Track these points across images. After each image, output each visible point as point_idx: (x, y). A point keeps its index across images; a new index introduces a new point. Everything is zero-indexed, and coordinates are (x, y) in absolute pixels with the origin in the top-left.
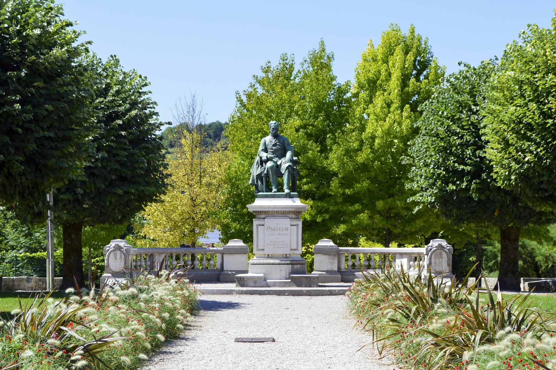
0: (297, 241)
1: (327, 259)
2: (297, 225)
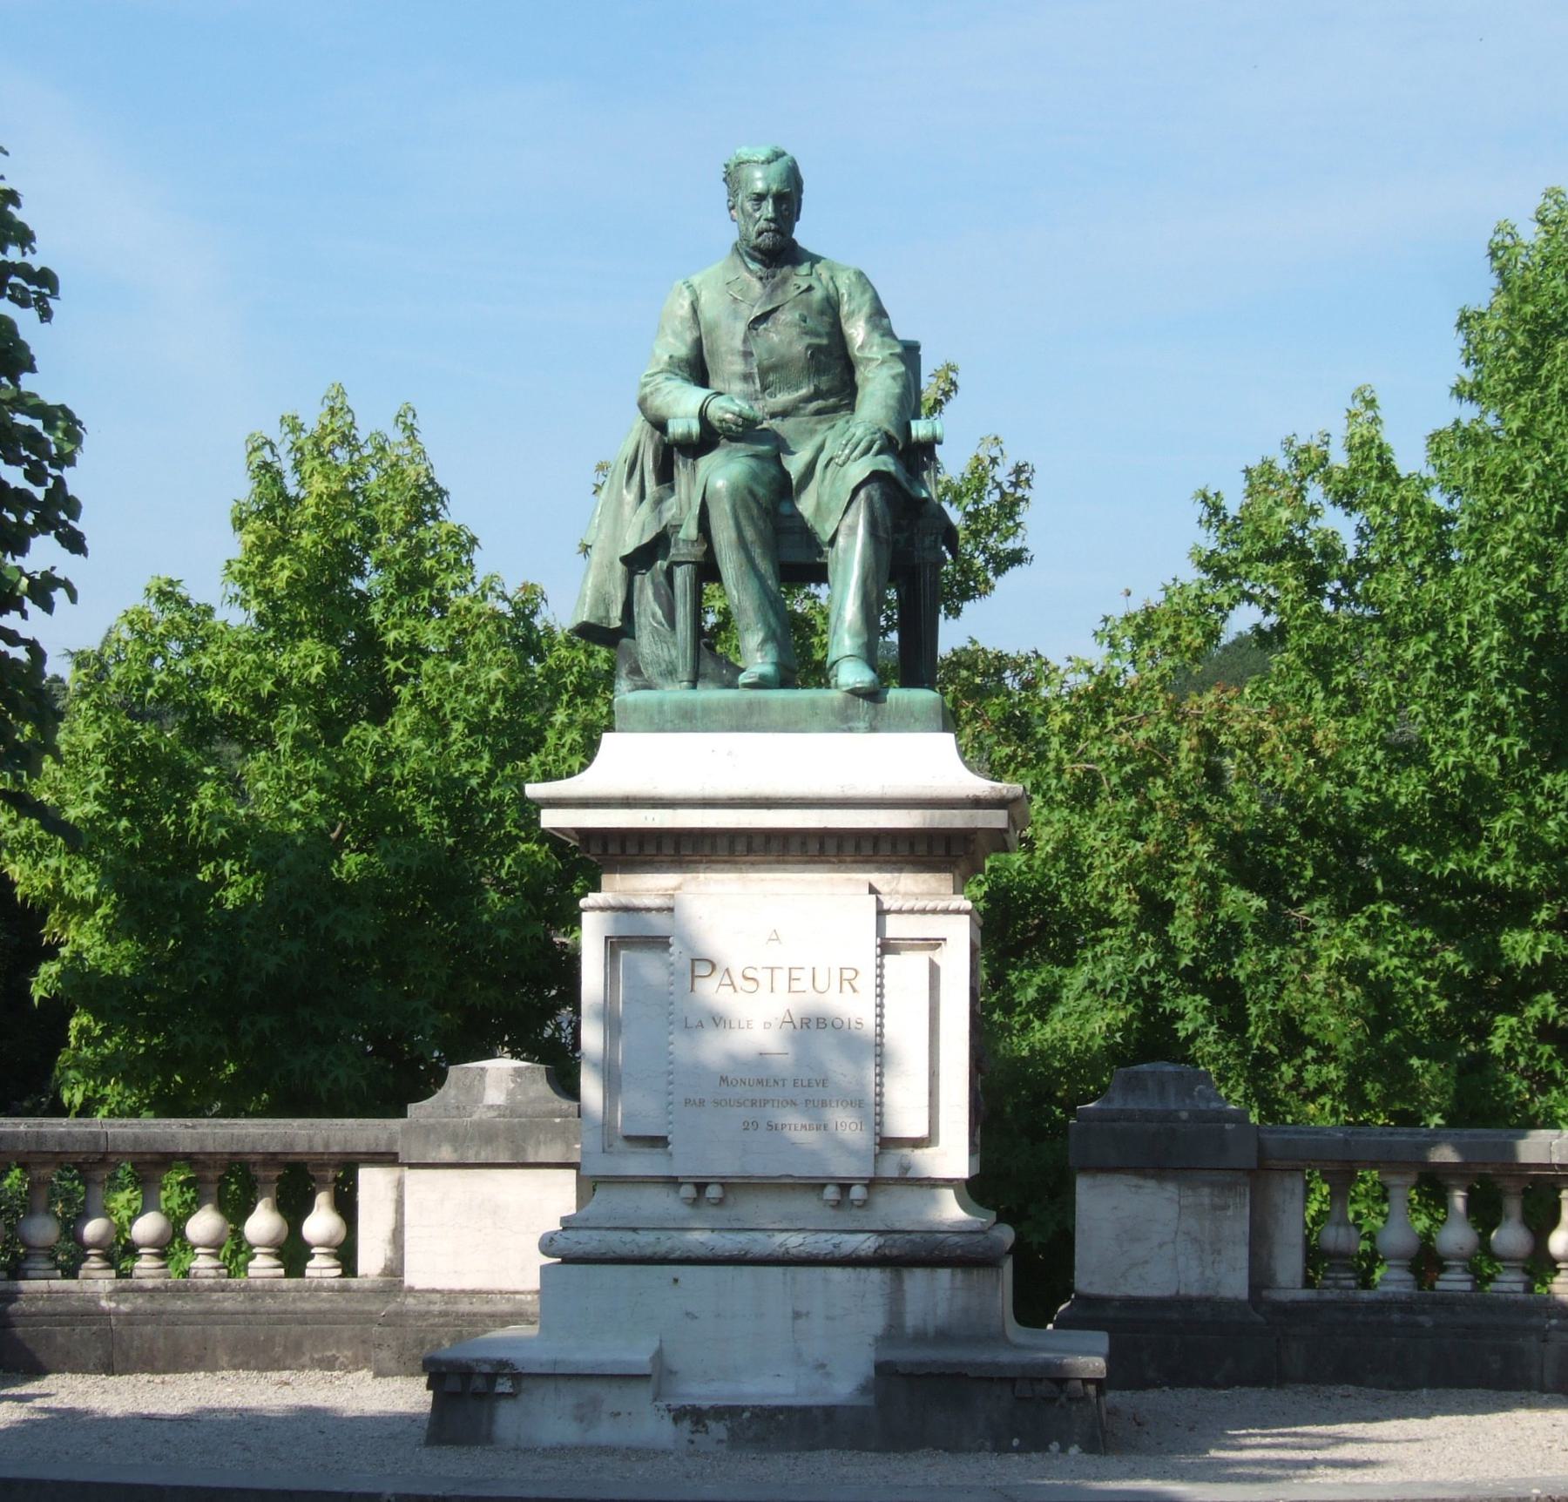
2: (935, 944)
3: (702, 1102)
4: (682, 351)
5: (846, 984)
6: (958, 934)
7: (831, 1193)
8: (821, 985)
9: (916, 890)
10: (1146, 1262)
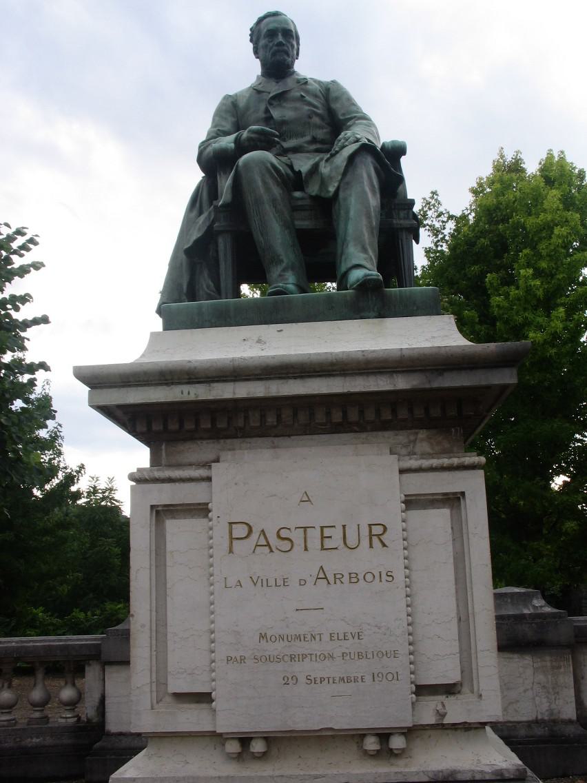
0: (464, 619)
1: (529, 672)
2: (454, 500)
3: (243, 659)
4: (227, 126)
5: (375, 540)
6: (474, 486)
7: (371, 744)
8: (352, 541)
9: (431, 452)
10: (518, 701)
